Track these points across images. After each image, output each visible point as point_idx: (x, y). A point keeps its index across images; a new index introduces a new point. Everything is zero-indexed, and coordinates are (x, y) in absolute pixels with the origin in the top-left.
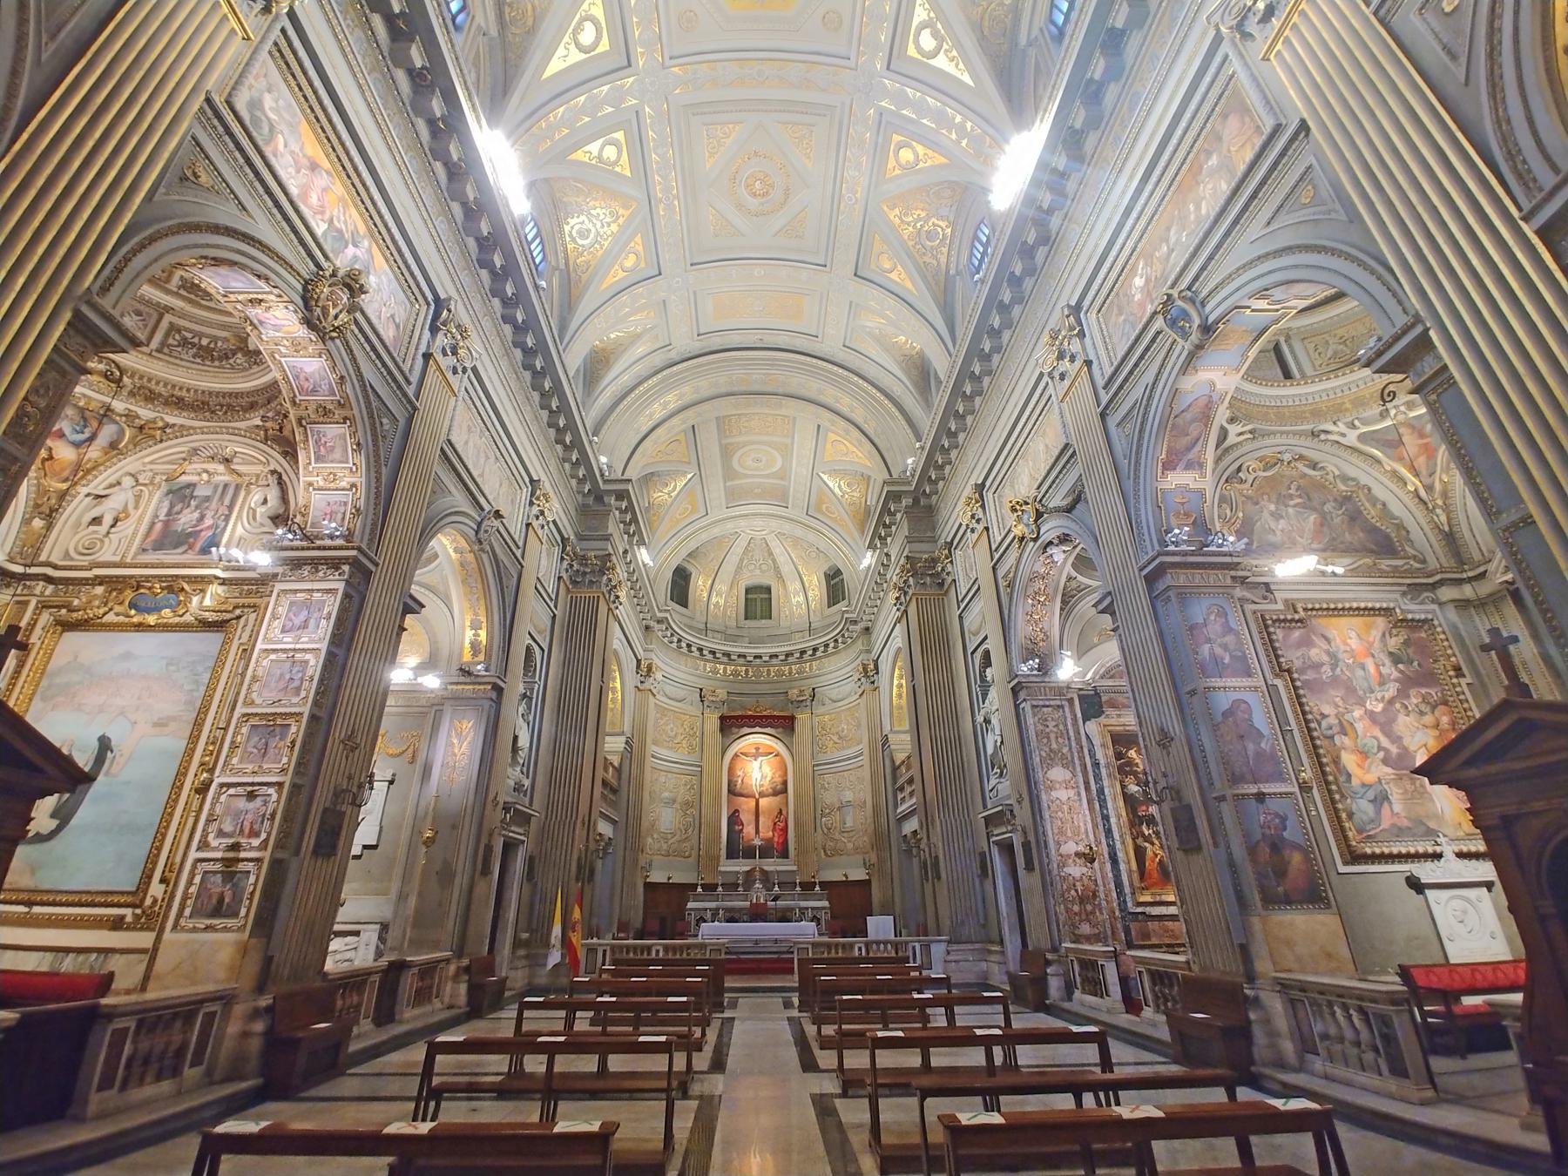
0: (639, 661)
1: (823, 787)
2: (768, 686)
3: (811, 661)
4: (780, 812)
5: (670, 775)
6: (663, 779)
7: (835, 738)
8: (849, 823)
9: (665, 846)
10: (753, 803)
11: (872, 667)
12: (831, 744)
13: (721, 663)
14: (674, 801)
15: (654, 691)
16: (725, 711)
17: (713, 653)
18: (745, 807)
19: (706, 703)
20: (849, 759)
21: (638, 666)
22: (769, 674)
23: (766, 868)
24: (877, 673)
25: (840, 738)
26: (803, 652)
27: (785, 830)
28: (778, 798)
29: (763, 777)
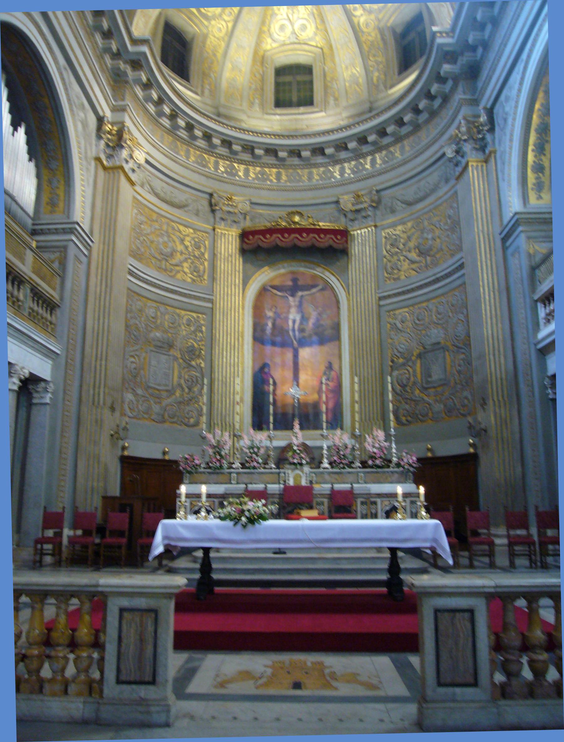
0: (100, 120)
1: (394, 327)
2: (310, 194)
3: (372, 153)
4: (330, 367)
5: (162, 308)
6: (151, 312)
7: (413, 255)
8: (437, 374)
9: (156, 408)
10: (289, 355)
11: (483, 119)
12: (406, 265)
13: (241, 162)
14: (171, 346)
15: (133, 177)
16: (248, 224)
17: (227, 143)
18: (278, 360)
19: (218, 215)
20: (437, 280)
21: (99, 128)
22: (310, 178)
23: (308, 443)
24: (492, 130)
25: (421, 253)
26: (362, 139)
27: (338, 390)
28: (326, 348)
29: (304, 319)
